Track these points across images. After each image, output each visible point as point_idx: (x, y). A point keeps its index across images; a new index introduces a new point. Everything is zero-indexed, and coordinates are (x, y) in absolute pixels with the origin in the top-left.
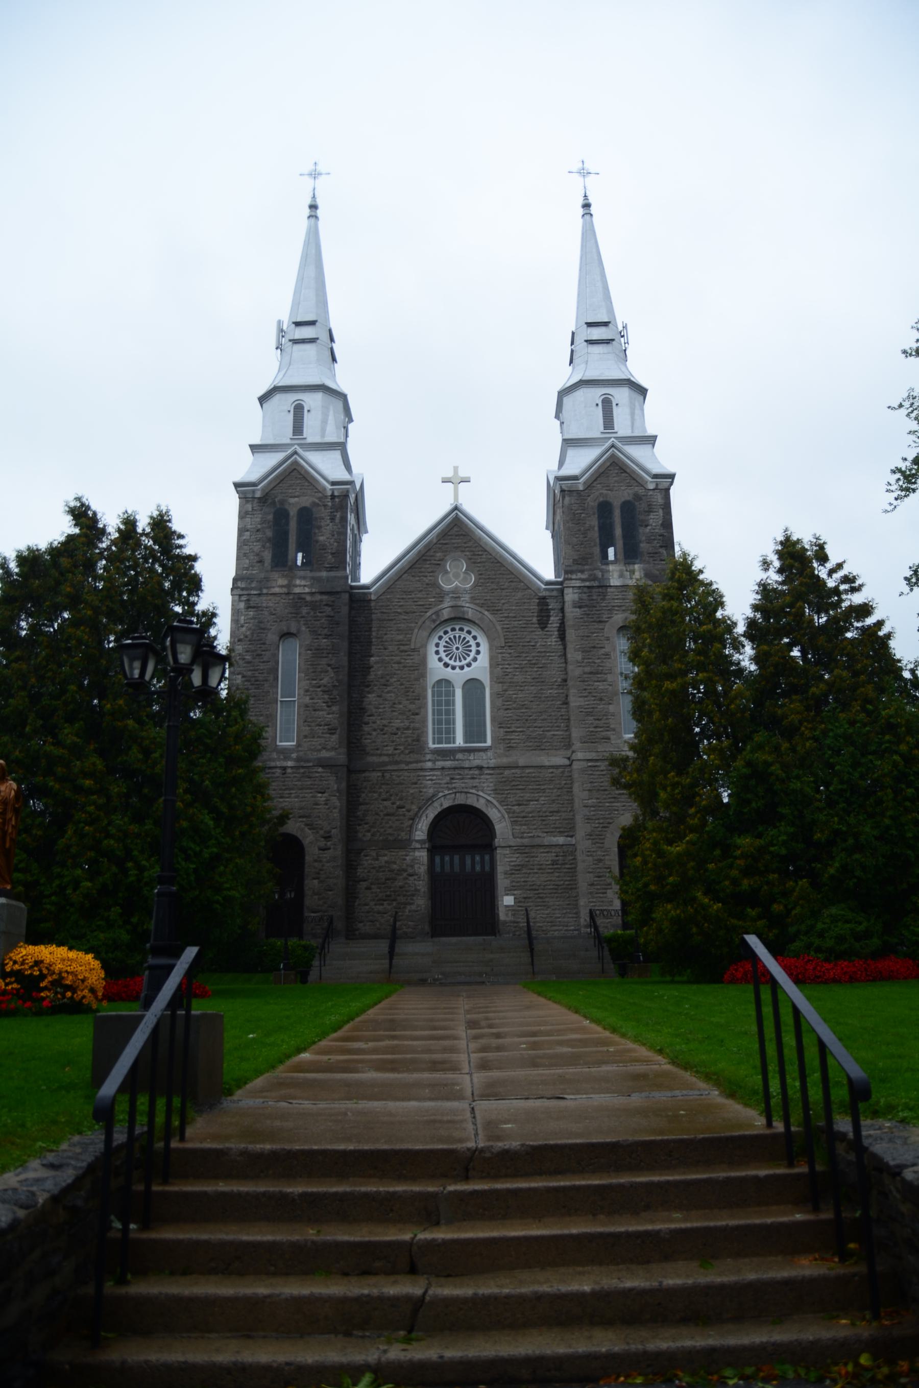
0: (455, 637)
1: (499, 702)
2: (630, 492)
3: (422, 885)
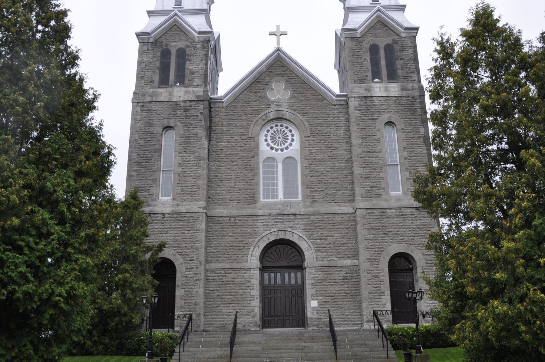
0: (277, 130)
3: (256, 293)
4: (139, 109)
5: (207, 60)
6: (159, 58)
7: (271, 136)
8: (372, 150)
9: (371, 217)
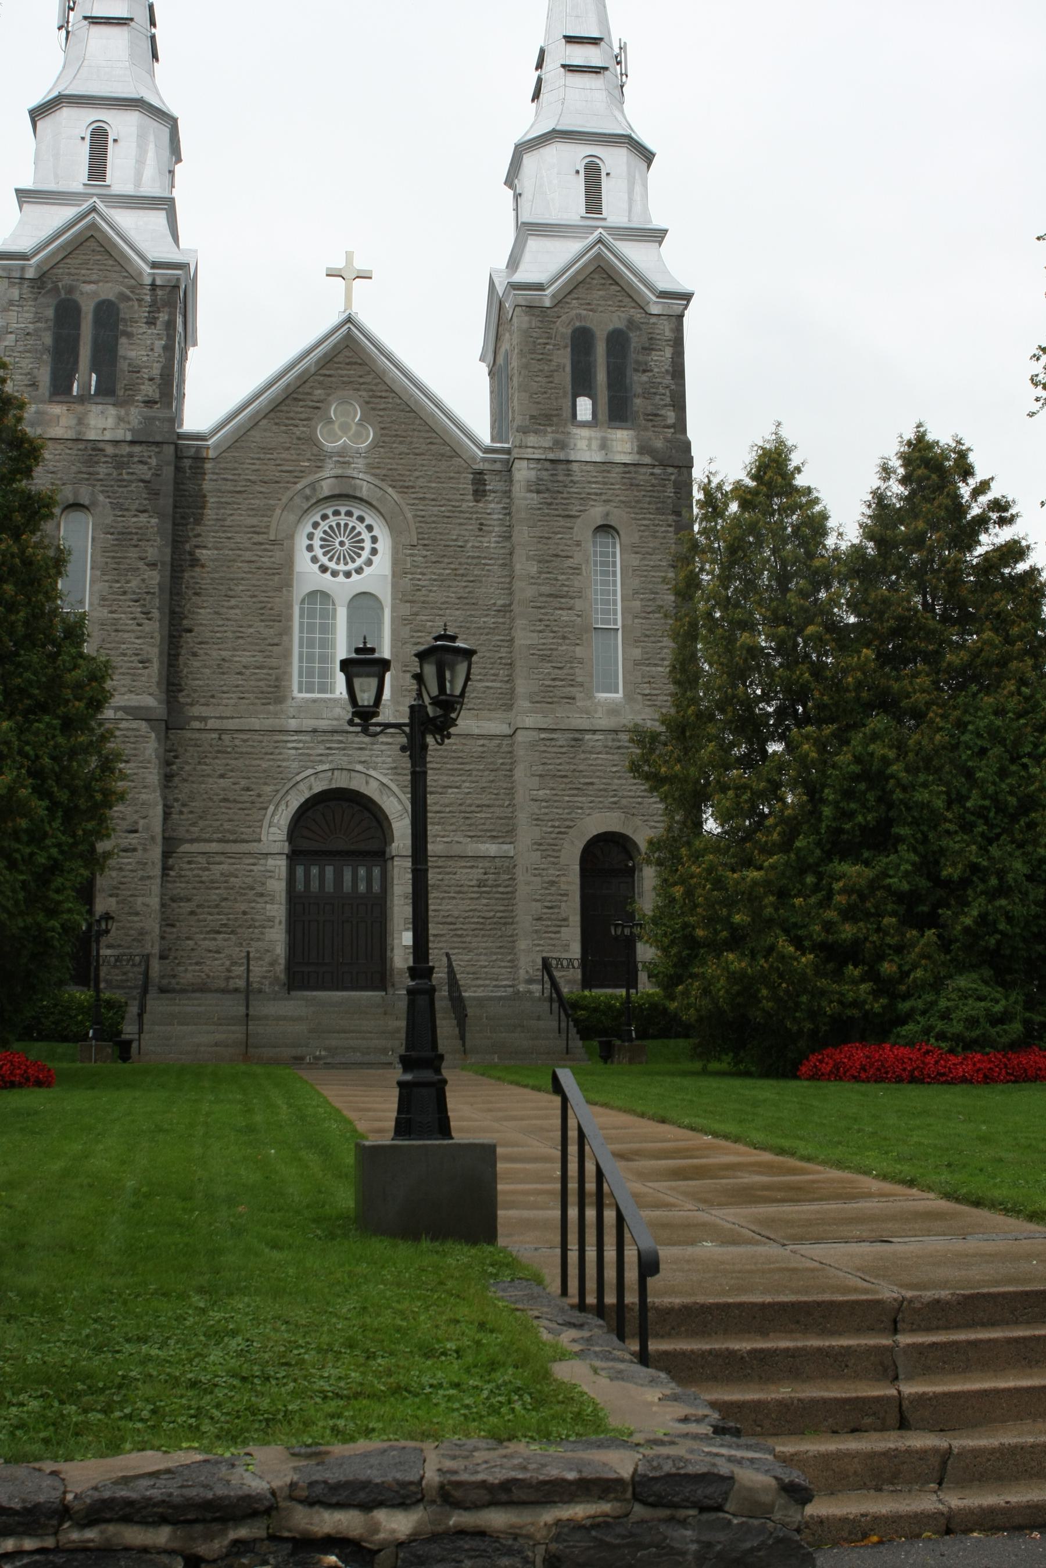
0: (338, 525)
2: (623, 315)
3: (278, 910)
6: (51, 324)
7: (322, 539)
8: (560, 592)
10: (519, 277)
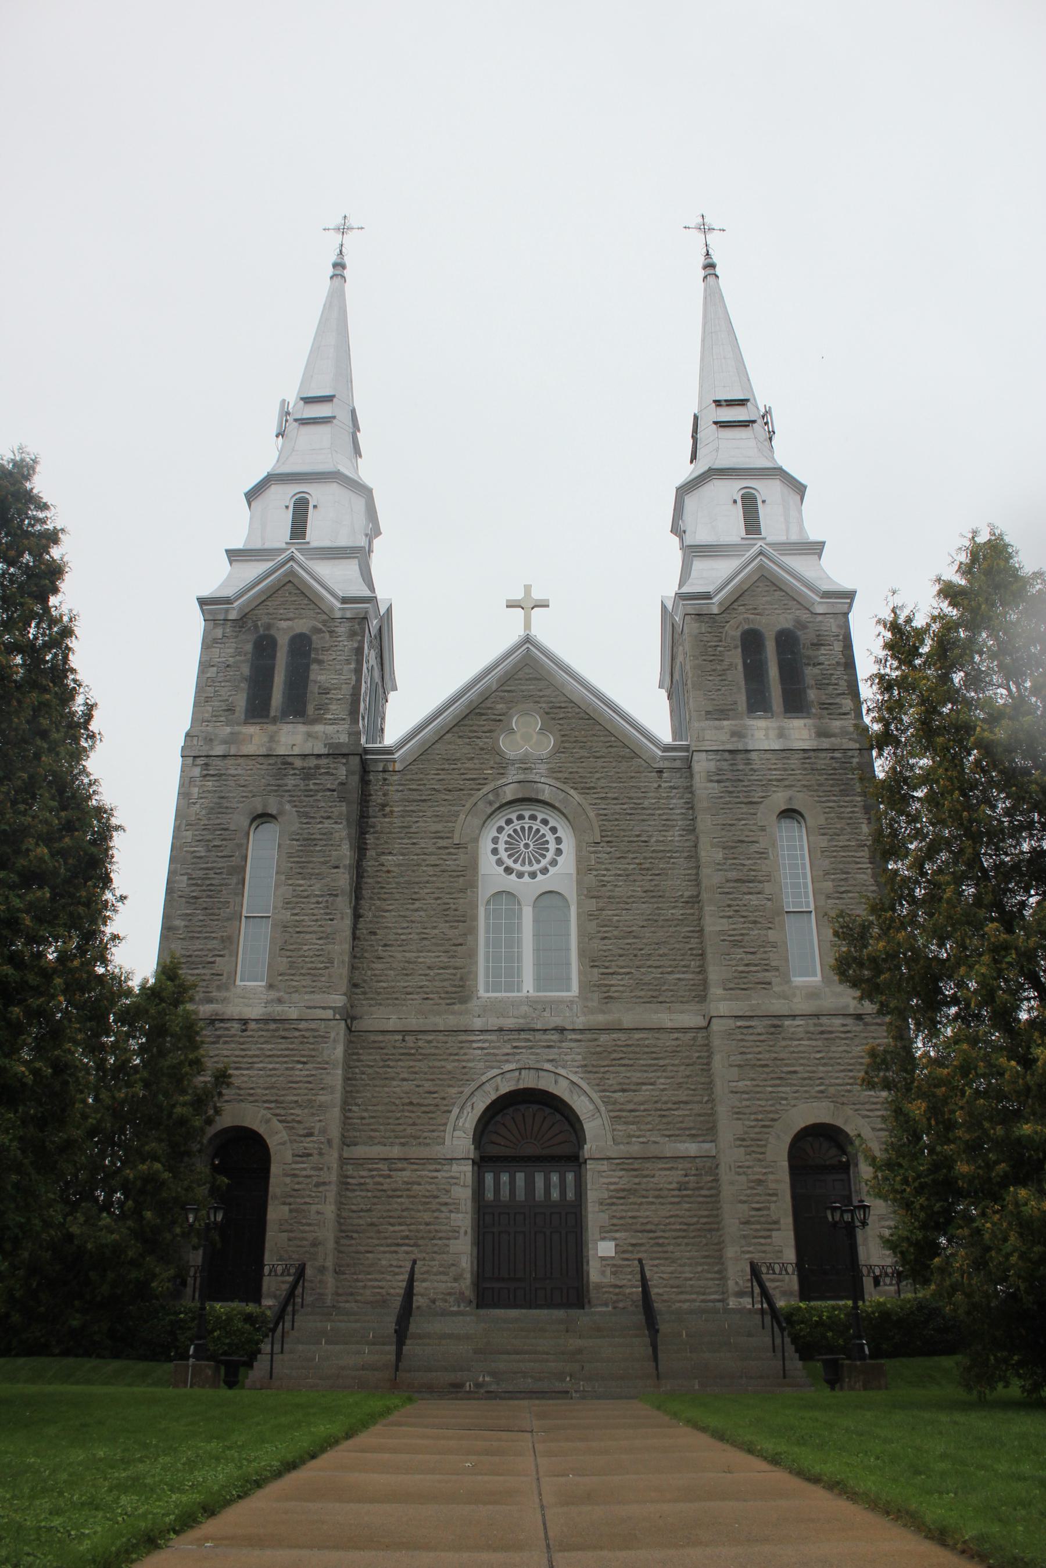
0: (523, 828)
1: (592, 927)
2: (790, 617)
3: (463, 1219)
4: (197, 771)
5: (359, 663)
7: (506, 843)
8: (750, 876)
9: (747, 1038)
10: (685, 589)
